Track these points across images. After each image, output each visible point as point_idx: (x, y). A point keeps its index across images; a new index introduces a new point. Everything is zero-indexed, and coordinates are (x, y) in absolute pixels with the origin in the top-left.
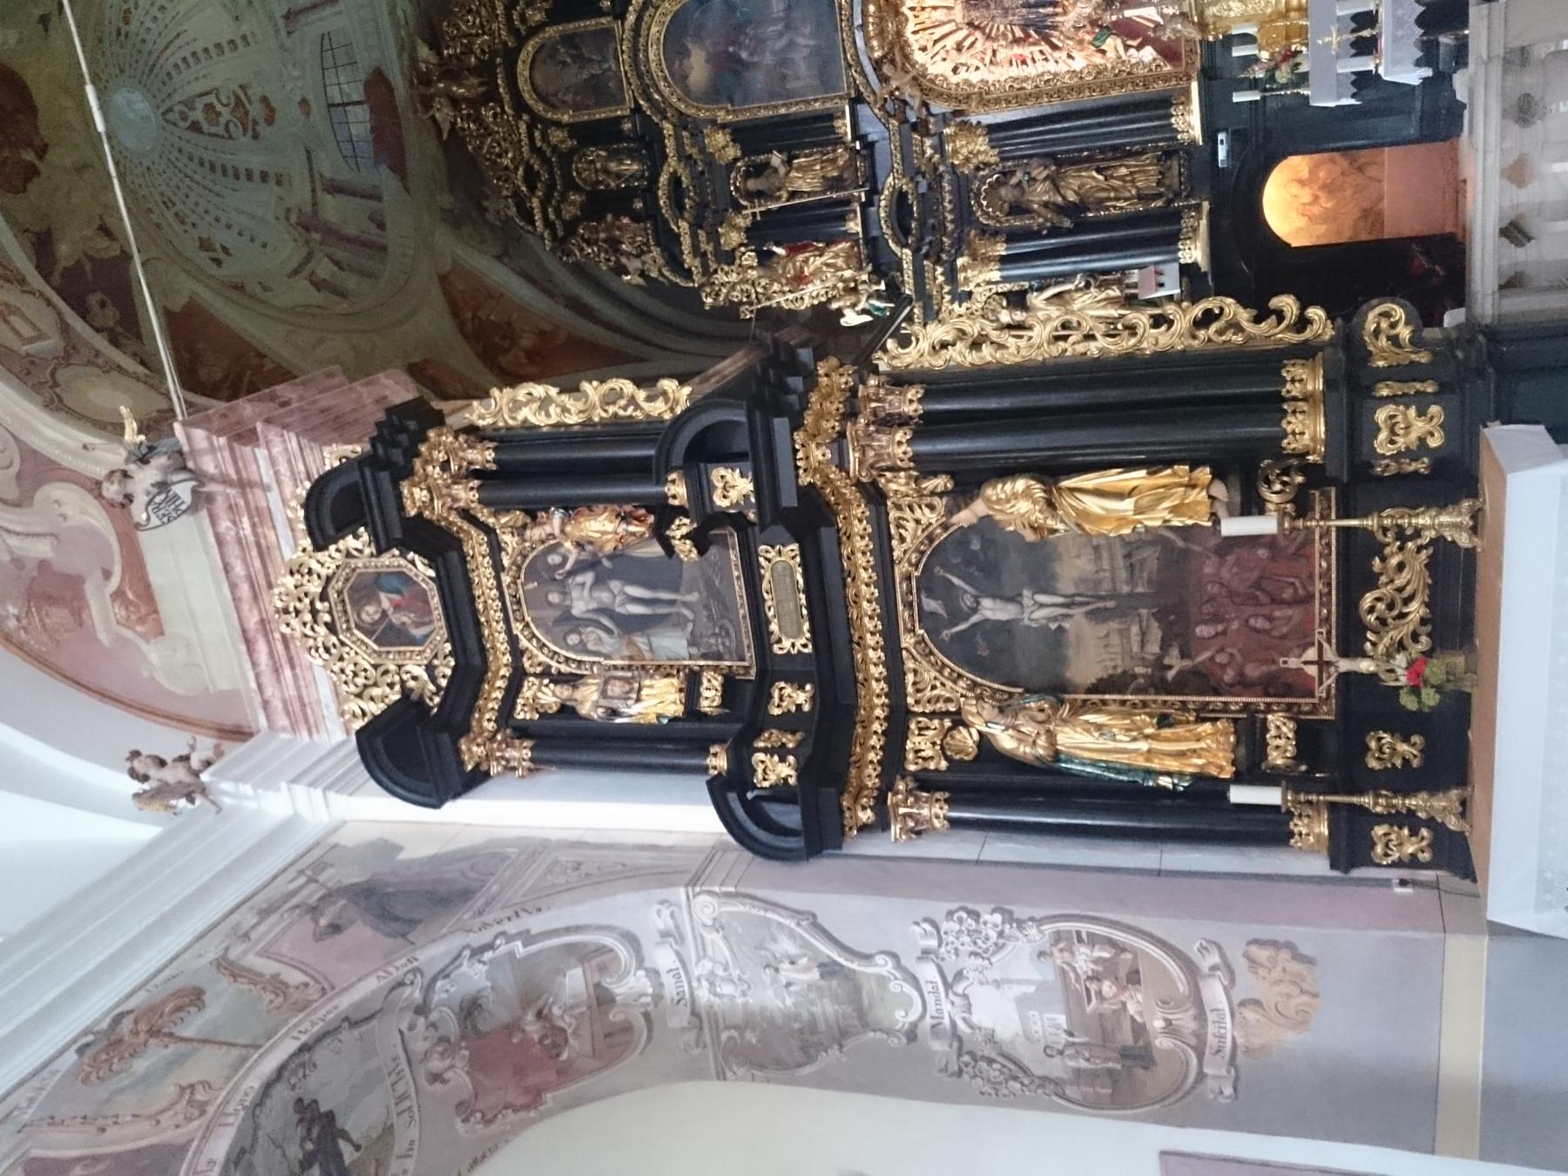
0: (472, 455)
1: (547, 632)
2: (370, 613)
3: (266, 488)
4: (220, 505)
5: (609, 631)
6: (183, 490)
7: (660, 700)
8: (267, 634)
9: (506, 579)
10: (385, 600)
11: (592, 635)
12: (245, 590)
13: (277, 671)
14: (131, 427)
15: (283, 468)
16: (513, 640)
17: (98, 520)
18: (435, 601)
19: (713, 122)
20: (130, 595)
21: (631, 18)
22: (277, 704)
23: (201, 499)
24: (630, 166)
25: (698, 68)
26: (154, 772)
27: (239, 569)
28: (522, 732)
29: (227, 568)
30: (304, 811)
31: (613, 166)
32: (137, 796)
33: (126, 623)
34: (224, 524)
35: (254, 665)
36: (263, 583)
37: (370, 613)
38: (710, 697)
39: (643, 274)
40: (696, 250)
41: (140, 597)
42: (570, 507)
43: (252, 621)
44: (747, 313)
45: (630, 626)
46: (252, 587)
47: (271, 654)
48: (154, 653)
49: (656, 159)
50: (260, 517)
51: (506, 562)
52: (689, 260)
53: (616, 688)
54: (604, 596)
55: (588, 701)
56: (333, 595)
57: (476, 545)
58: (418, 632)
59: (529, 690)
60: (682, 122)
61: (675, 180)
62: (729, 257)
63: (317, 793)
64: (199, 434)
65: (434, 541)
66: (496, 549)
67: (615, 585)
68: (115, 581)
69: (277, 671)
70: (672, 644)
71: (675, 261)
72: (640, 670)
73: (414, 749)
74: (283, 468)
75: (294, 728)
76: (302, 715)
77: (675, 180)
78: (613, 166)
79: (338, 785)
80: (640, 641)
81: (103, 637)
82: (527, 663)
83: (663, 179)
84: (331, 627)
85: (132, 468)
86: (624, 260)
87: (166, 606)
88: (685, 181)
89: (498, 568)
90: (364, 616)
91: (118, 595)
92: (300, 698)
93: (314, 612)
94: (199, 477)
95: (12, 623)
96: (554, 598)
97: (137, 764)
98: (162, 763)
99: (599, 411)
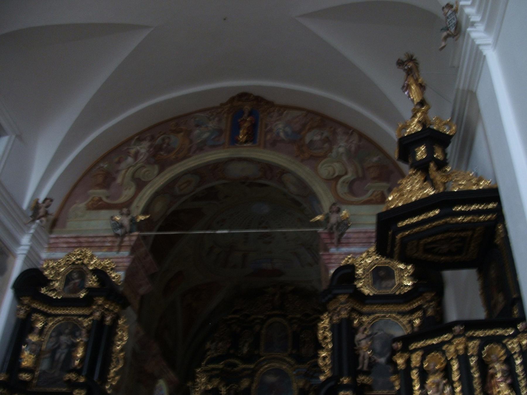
0: (108, 319)
1: (57, 327)
2: (75, 275)
3: (119, 251)
4: (114, 239)
5: (54, 345)
6: (119, 231)
7: (27, 359)
8: (77, 243)
9: (75, 318)
10: (77, 281)
11: (53, 340)
12: (91, 240)
13: (67, 243)
14: (142, 218)
15: (120, 260)
16: (57, 316)
17: (123, 199)
18: (73, 296)
19: (252, 382)
20: (100, 203)
21: (288, 359)
22: (57, 241)
23: (117, 235)
24: (245, 350)
25: (271, 379)
26: (45, 205)
27: (97, 240)
28: (29, 315)
29: (97, 237)
30: (22, 247)
31: (247, 345)
32: (38, 199)
33: (92, 200)
34: (109, 239)
35: (68, 238)
36: (92, 245)
37: (75, 275)
38: (25, 376)
39: (209, 349)
40: (213, 369)
41: (98, 206)
42: (86, 345)
43: (82, 240)
44: (190, 384)
45: (53, 352)
46: (91, 242)
47: (71, 243)
48: (82, 205)
49: (248, 359)
50: (110, 249)
51: (80, 319)
52: (211, 366)
53: (34, 347)
54: (63, 347)
55: (33, 338)
56: (83, 266)
57: (86, 312)
58: (67, 287)
59: (41, 317)
60: (254, 371)
61: (235, 365)
62: (209, 380)
63: (25, 252)
64: (134, 238)
65: (88, 302)
66: (85, 316)
67: (66, 351)
68: (105, 199)
69: (67, 243)
70: (45, 365)
71: (212, 361)
72: (39, 355)
73: (31, 283)
74: (120, 260)
75: (49, 244)
76: (52, 247)
77: (235, 365)
78: (247, 345)
79: (28, 258)
80: (48, 355)
81: (91, 191)
82: (50, 319)
83: (237, 362)
84: (74, 263)
85: (130, 217)
86: (214, 344)
87: (94, 213)
88: (236, 369)
89: (80, 316)
90: (75, 274)
91: (100, 199)
92: (57, 247)
93: (80, 259)
94: (123, 236)
95: (102, 165)
96: (67, 331)
97: (48, 201)
98: (47, 207)
99: (115, 356)
